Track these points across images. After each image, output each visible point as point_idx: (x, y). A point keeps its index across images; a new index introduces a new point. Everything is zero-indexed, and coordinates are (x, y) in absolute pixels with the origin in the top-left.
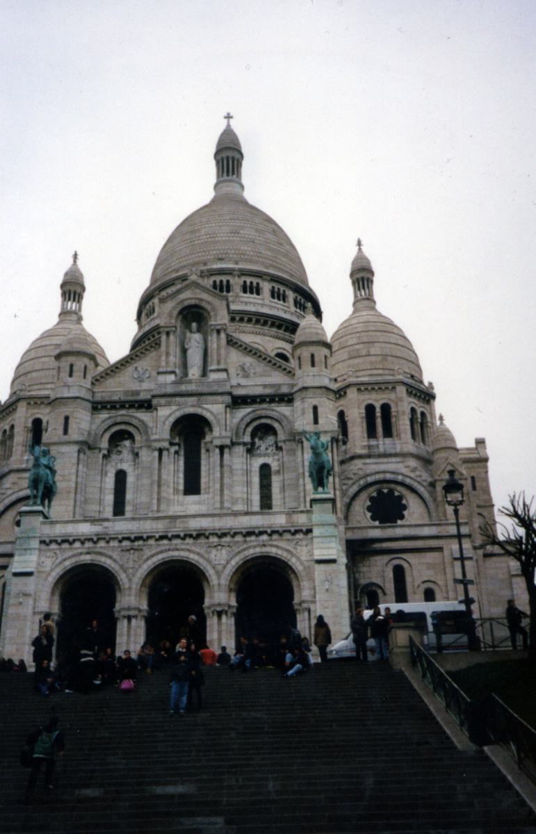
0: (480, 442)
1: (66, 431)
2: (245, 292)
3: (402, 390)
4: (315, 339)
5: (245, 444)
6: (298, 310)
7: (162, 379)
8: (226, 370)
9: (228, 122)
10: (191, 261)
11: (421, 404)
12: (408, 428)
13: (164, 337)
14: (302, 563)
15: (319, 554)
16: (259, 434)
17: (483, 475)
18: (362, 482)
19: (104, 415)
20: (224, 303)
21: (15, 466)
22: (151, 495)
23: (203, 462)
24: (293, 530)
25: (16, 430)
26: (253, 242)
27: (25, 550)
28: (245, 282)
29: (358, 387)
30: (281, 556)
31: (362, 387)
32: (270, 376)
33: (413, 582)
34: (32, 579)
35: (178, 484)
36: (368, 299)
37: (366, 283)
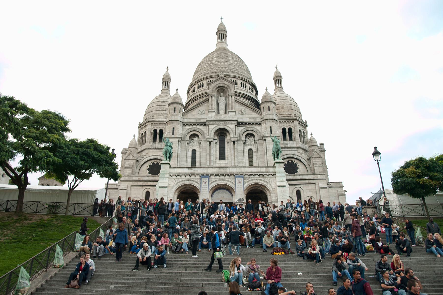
1: (173, 134)
3: (296, 123)
4: (269, 100)
5: (242, 140)
6: (251, 92)
7: (210, 114)
8: (235, 112)
9: (222, 20)
10: (210, 71)
11: (303, 128)
13: (210, 98)
14: (272, 187)
15: (279, 184)
16: (248, 137)
17: (323, 157)
19: (187, 127)
21: (148, 147)
22: (207, 159)
23: (226, 147)
24: (268, 174)
25: (147, 133)
26: (234, 65)
27: (163, 178)
28: (231, 80)
30: (263, 184)
32: (252, 114)
33: (304, 196)
34: (166, 189)
35: (217, 155)
36: (281, 88)
37: (280, 81)
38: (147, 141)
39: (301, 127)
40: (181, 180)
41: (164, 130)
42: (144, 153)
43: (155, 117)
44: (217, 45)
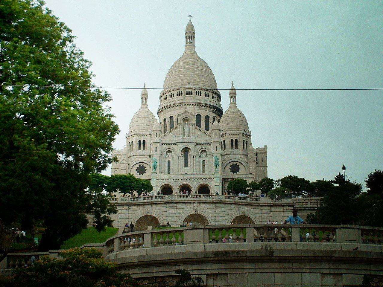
0: (266, 147)
2: (196, 95)
5: (199, 155)
6: (213, 99)
9: (190, 19)
11: (246, 138)
12: (243, 146)
13: (179, 126)
16: (202, 152)
18: (229, 162)
19: (165, 146)
20: (194, 117)
23: (189, 159)
28: (196, 91)
29: (229, 134)
31: (230, 134)
34: (155, 187)
38: (135, 150)
39: (245, 138)
40: (163, 182)
41: (146, 141)
42: (133, 158)
43: (139, 131)
44: (185, 47)
